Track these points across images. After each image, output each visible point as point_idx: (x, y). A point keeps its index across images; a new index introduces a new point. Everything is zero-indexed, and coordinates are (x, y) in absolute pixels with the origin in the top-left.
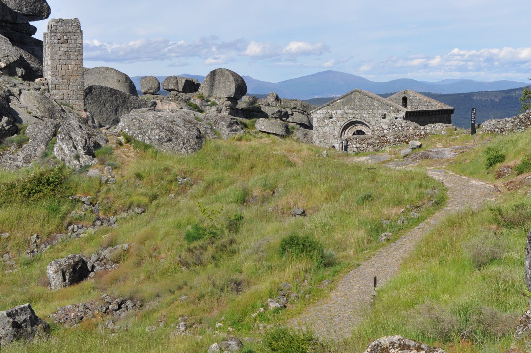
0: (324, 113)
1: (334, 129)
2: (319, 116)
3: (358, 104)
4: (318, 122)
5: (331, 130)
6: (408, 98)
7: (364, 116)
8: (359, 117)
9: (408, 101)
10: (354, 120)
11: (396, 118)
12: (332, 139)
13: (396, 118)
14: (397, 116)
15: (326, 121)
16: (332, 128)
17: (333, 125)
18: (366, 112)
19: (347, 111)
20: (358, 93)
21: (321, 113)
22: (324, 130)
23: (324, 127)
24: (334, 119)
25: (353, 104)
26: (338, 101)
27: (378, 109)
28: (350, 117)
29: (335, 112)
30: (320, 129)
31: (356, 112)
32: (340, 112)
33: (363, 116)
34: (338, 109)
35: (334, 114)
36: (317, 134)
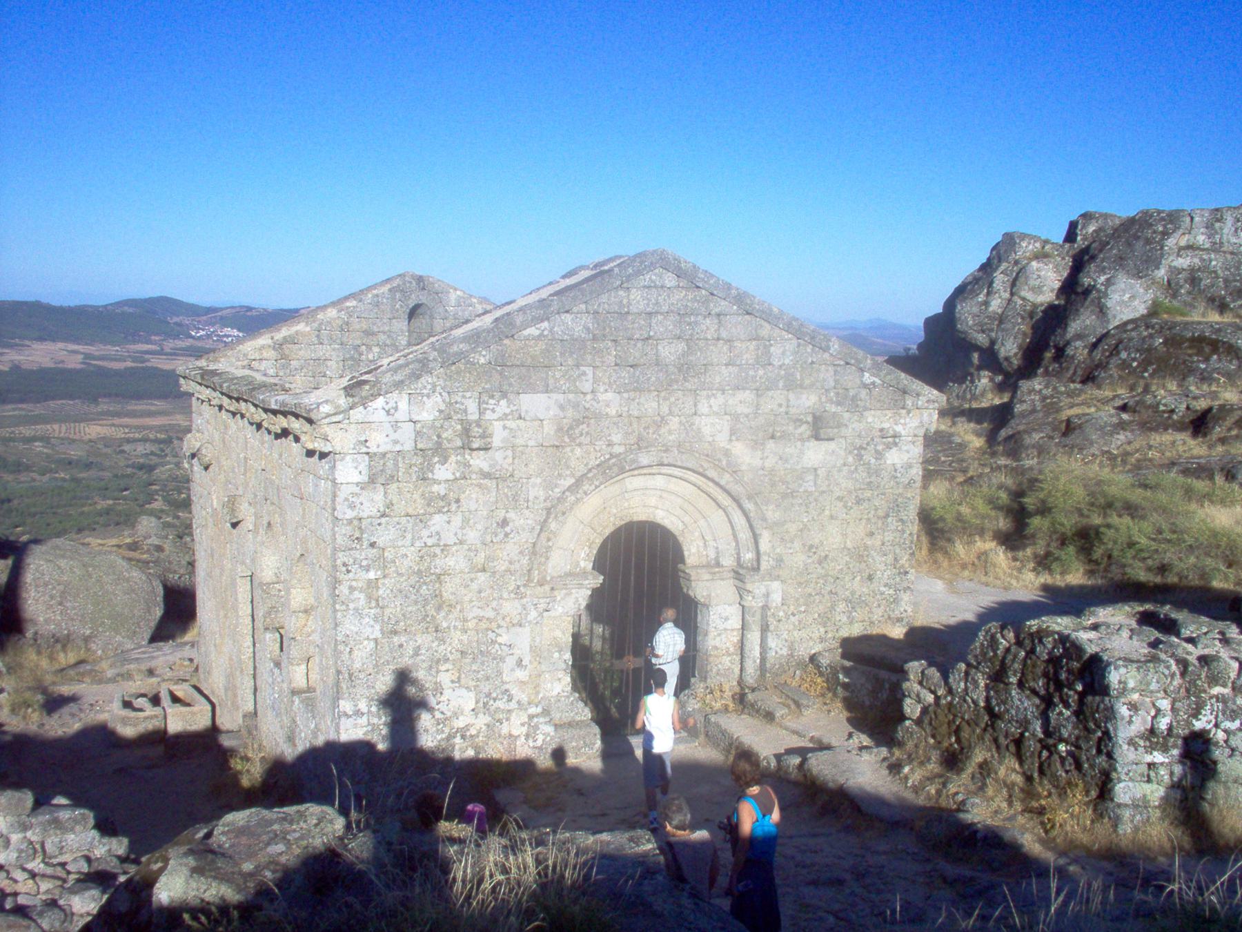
2: (379, 441)
3: (669, 351)
5: (472, 536)
15: (443, 472)
20: (670, 280)
23: (422, 520)
25: (635, 353)
27: (792, 385)
28: (616, 438)
36: (372, 575)
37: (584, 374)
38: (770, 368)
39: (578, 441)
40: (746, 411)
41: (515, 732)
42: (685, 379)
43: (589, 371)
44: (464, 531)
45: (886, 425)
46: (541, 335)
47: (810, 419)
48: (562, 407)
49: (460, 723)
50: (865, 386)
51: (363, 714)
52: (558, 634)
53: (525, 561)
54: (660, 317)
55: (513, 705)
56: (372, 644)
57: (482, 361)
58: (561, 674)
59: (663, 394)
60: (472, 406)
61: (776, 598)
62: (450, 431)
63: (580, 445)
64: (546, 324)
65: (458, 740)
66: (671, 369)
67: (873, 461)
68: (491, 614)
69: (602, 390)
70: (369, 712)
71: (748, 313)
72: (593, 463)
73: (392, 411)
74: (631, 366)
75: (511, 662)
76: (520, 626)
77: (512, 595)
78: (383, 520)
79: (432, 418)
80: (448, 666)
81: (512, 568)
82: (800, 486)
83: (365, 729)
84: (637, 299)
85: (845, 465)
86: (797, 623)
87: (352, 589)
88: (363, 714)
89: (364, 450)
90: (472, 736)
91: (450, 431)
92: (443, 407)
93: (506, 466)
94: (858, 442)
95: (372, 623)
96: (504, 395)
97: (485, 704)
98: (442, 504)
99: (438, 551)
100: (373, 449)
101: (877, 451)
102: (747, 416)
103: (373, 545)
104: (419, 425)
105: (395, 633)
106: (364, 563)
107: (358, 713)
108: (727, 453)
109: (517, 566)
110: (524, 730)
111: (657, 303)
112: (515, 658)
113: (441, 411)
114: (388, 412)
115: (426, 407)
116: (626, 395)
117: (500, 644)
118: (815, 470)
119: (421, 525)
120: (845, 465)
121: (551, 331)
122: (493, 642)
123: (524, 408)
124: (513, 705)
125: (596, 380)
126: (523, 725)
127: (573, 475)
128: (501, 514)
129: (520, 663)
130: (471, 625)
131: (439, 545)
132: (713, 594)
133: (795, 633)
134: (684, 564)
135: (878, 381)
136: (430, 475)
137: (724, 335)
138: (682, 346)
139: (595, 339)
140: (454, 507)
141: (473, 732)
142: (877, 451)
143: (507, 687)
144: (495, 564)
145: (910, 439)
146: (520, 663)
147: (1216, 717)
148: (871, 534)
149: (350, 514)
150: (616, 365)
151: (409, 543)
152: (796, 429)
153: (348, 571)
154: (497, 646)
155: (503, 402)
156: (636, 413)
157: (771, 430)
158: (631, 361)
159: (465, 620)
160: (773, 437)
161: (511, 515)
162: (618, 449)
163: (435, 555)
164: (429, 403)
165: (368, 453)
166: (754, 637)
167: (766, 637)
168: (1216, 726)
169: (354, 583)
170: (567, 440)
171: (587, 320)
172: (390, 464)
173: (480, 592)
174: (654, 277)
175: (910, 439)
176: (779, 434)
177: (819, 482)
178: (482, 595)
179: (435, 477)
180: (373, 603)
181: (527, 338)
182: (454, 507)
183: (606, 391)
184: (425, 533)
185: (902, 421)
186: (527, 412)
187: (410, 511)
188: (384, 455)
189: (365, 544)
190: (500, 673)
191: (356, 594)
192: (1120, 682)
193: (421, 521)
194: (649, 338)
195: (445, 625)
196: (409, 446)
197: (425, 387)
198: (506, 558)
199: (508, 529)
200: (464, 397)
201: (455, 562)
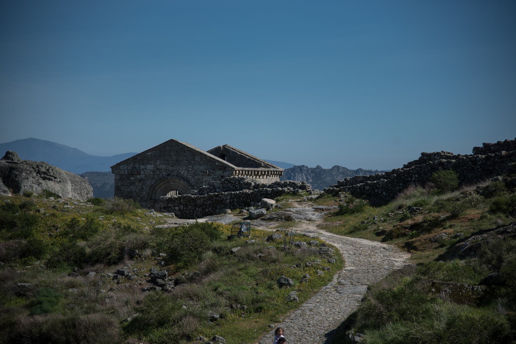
1: (143, 188)
5: (137, 191)
7: (182, 173)
21: (125, 168)
27: (200, 165)
28: (164, 174)
29: (142, 167)
31: (171, 168)
33: (180, 173)
35: (143, 169)
40: (190, 169)
43: (159, 161)
45: (221, 173)
48: (154, 168)
53: (147, 195)
64: (151, 153)
94: (215, 177)
96: (143, 165)
103: (120, 190)
109: (145, 196)
121: (152, 154)
125: (160, 163)
128: (142, 186)
137: (185, 154)
142: (219, 179)
155: (143, 166)
160: (196, 175)
161: (144, 187)
172: (123, 176)
184: (129, 189)
188: (123, 175)
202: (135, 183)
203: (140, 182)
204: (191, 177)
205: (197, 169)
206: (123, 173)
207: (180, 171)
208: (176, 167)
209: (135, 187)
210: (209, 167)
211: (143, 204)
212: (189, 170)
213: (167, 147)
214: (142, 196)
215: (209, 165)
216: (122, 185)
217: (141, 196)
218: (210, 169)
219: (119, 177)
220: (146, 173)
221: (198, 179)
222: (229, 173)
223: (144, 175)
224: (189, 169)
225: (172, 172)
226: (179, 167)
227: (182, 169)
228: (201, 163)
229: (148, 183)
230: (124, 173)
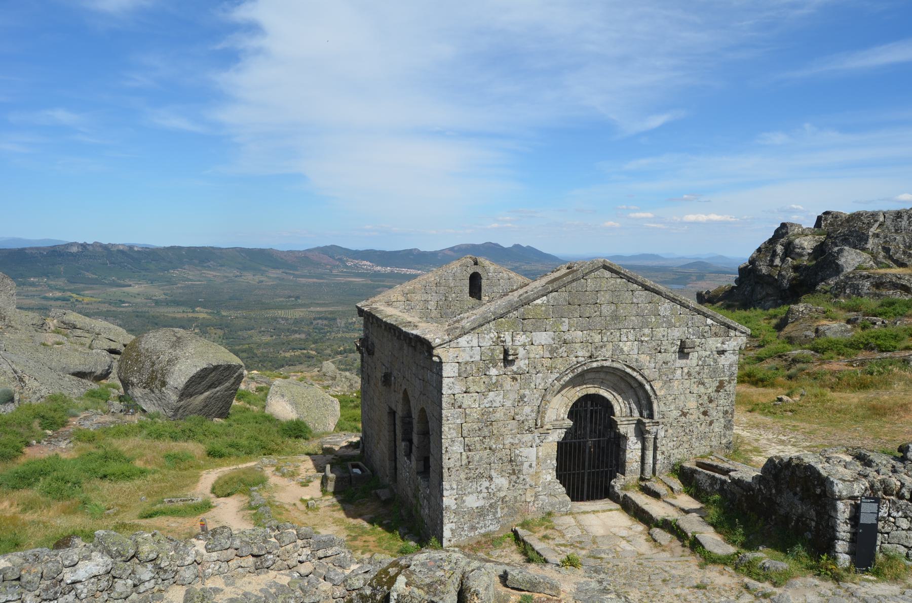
0: (487, 342)
1: (522, 397)
2: (464, 357)
3: (607, 310)
4: (463, 375)
5: (508, 404)
6: (483, 275)
7: (625, 349)
8: (609, 354)
9: (484, 282)
10: (595, 365)
11: (722, 352)
12: (514, 436)
13: (722, 352)
14: (725, 347)
15: (493, 372)
16: (513, 396)
17: (517, 386)
18: (631, 337)
19: (567, 336)
20: (607, 274)
21: (475, 343)
22: (486, 403)
24: (521, 364)
25: (588, 311)
26: (539, 301)
27: (670, 326)
28: (579, 354)
29: (521, 338)
30: (467, 401)
31: (597, 338)
32: (543, 338)
33: (622, 351)
34: (537, 329)
35: (524, 346)
36: (459, 421)
37: (564, 322)
38: (658, 317)
39: (560, 355)
40: (646, 339)
41: (528, 500)
42: (615, 324)
44: (504, 400)
45: (719, 345)
46: (543, 303)
47: (679, 343)
48: (554, 339)
49: (502, 494)
50: (707, 325)
51: (454, 489)
52: (550, 450)
53: (534, 415)
54: (602, 293)
55: (527, 486)
56: (459, 456)
57: (514, 316)
58: (551, 471)
59: (603, 331)
60: (508, 338)
61: (662, 434)
62: (498, 351)
63: (561, 357)
64: (545, 298)
65: (500, 503)
66: (608, 318)
67: (712, 363)
68: (517, 441)
69: (573, 329)
70: (457, 488)
71: (646, 290)
72: (567, 367)
73: (470, 342)
74: (588, 318)
75: (526, 465)
76: (531, 447)
77: (527, 432)
78: (465, 395)
79: (489, 344)
80: (496, 466)
81: (528, 418)
82: (674, 376)
83: (455, 497)
84: (590, 283)
85: (697, 365)
86: (672, 447)
87: (450, 428)
88: (454, 489)
89: (456, 361)
90: (506, 501)
91: (498, 351)
92: (495, 340)
93: (525, 368)
95: (459, 445)
96: (524, 332)
97: (513, 486)
98: (493, 386)
99: (491, 410)
100: (460, 361)
101: (714, 359)
102: (646, 342)
103: (460, 407)
104: (483, 348)
105: (470, 450)
106: (456, 416)
107: (452, 489)
108: (637, 360)
110: (533, 499)
111: (601, 285)
112: (530, 463)
113: (493, 342)
114: (468, 342)
115: (486, 340)
116: (585, 332)
117: (521, 456)
118: (682, 368)
119: (483, 397)
120: (697, 365)
121: (548, 301)
122: (518, 455)
123: (534, 339)
124: (527, 486)
125: (570, 326)
126: (532, 496)
127: (557, 372)
128: (522, 391)
129: (530, 466)
130: (507, 447)
131: (492, 407)
132: (629, 431)
133: (671, 451)
134: (614, 416)
135: (715, 323)
136: (488, 373)
137: (635, 300)
138: (613, 307)
139: (569, 304)
140: (499, 388)
141: (507, 499)
142: (714, 359)
143: (525, 477)
144: (519, 416)
145: (732, 352)
146: (530, 466)
147: (889, 510)
148: (711, 401)
149: (450, 392)
150: (580, 317)
151: (477, 406)
152: (672, 347)
153: (448, 420)
154: (520, 457)
156: (590, 341)
157: (659, 349)
158: (588, 315)
159: (504, 445)
160: (660, 352)
161: (527, 392)
162: (581, 359)
163: (490, 412)
164: (487, 337)
165: (458, 363)
166: (650, 454)
167: (656, 453)
168: (889, 515)
169: (451, 426)
170: (555, 354)
171: (565, 295)
172: (468, 368)
173: (511, 430)
174: (599, 273)
175: (732, 352)
176: (663, 351)
177: (684, 374)
178: (513, 432)
179: (490, 374)
180: (460, 435)
181: (536, 305)
182: (499, 388)
183: (575, 330)
184: (486, 401)
185: (727, 343)
186: (536, 341)
187: (479, 391)
188: (466, 363)
189: (456, 406)
190: (520, 471)
191: (452, 431)
192: (839, 492)
193: (483, 395)
194: (596, 303)
195: (494, 446)
196: (477, 358)
197: (485, 330)
198: (525, 414)
199: (525, 400)
200: (505, 334)
201: (499, 415)
202: (501, 386)
203: (517, 380)
204: (648, 358)
205: (664, 336)
206: (468, 359)
207: (621, 344)
208: (611, 333)
209: (501, 396)
210: (690, 330)
211: (524, 440)
212: (642, 342)
213: (589, 280)
214: (522, 419)
215: (690, 325)
216: (465, 392)
217: (517, 417)
218: (694, 335)
219: (457, 371)
220: (532, 356)
221: (664, 363)
222: (735, 343)
223: (527, 362)
224: (642, 339)
225: (601, 347)
226: (618, 334)
227: (625, 339)
228: (673, 321)
229: (538, 381)
230: (471, 357)
